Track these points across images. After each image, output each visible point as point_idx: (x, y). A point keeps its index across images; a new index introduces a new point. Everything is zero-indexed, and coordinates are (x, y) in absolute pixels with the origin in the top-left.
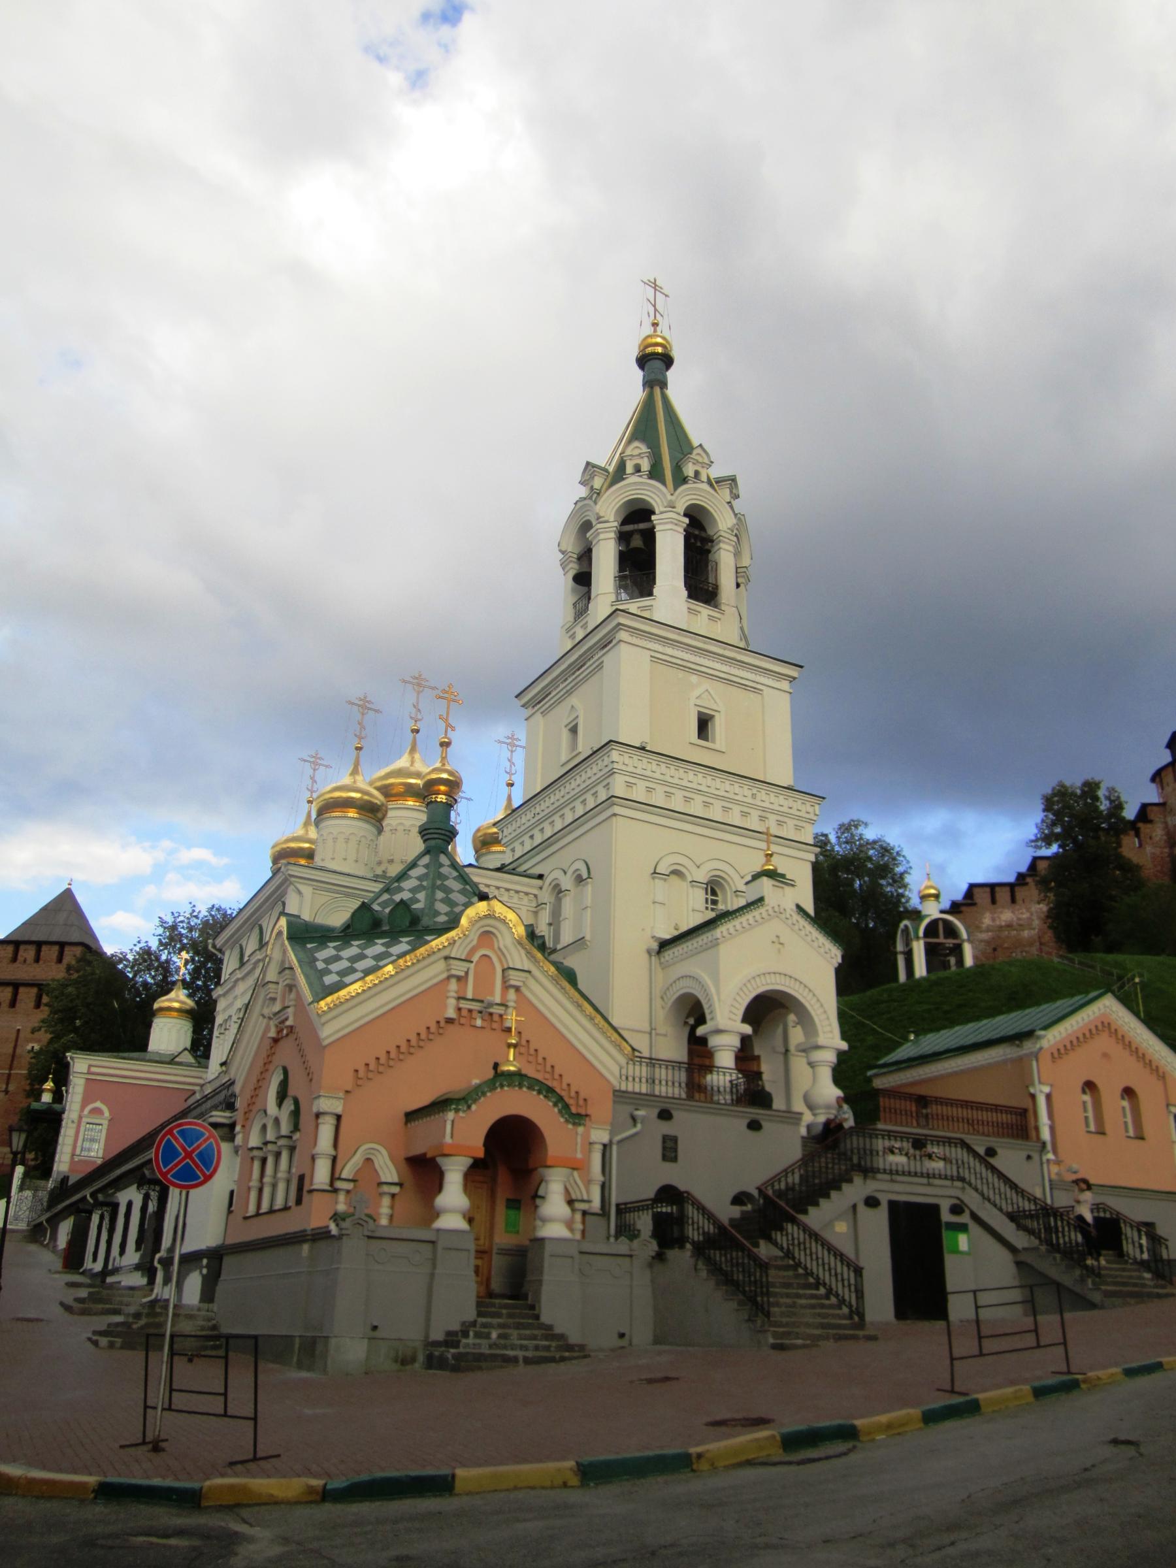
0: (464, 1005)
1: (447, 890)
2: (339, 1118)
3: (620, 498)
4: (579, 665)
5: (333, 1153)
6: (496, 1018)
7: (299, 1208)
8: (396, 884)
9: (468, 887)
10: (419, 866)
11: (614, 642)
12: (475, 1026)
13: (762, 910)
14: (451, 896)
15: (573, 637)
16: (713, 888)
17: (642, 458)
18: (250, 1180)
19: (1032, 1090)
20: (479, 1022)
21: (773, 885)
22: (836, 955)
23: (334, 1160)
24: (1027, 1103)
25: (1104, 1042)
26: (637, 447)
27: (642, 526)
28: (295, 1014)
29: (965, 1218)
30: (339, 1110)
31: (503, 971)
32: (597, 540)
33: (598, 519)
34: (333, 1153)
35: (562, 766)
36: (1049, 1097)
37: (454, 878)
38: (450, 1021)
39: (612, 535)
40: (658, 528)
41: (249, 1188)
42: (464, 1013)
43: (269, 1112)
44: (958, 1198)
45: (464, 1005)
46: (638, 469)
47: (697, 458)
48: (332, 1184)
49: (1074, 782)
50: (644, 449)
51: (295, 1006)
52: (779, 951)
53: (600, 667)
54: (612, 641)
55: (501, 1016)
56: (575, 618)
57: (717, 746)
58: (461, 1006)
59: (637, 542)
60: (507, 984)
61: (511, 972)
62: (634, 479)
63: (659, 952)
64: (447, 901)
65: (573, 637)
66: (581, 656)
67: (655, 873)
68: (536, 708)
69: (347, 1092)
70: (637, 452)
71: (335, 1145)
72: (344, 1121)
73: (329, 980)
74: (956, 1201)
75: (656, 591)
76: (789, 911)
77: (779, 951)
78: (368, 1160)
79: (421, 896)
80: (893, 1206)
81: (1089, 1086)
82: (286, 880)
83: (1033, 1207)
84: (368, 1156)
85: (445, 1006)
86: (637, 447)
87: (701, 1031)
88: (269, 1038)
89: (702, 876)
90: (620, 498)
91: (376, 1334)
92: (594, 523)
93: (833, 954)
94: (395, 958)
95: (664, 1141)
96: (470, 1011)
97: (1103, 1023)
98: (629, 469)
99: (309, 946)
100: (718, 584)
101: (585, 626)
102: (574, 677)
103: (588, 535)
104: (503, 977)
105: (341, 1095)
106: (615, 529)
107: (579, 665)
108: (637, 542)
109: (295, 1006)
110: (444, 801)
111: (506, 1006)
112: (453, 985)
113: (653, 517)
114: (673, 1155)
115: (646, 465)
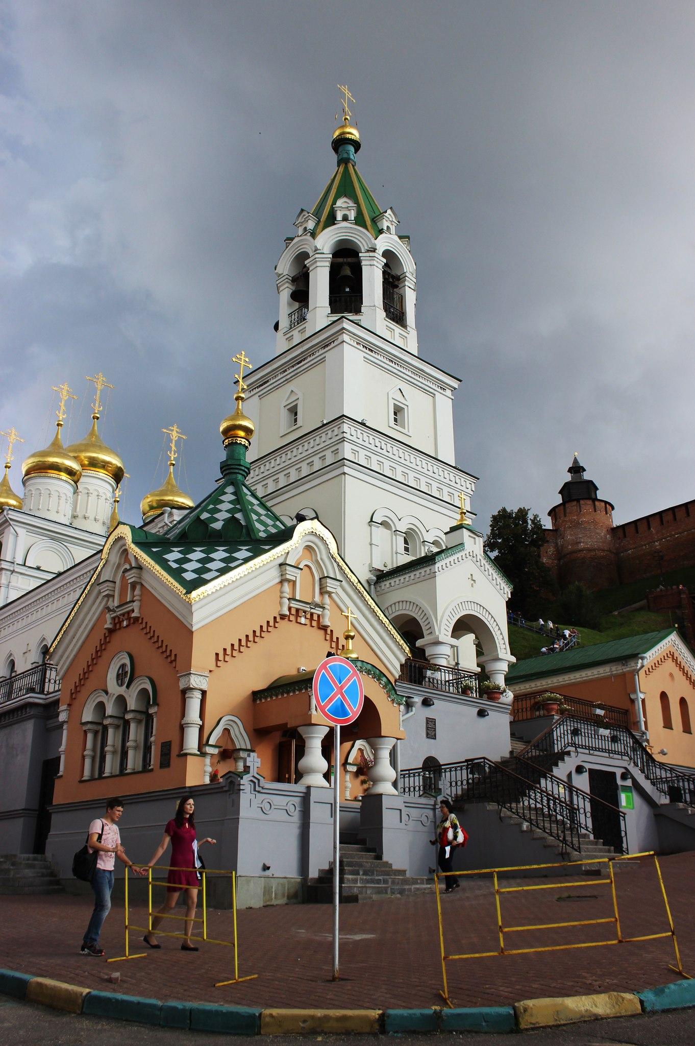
0: (294, 605)
2: (204, 693)
3: (337, 235)
4: (298, 360)
5: (201, 723)
6: (315, 617)
7: (166, 770)
9: (269, 513)
11: (336, 343)
12: (300, 623)
13: (463, 553)
14: (261, 518)
15: (290, 339)
16: (409, 537)
17: (350, 210)
18: (84, 750)
19: (633, 696)
20: (303, 620)
21: (469, 536)
22: (507, 592)
23: (201, 729)
24: (626, 705)
25: (669, 665)
26: (346, 202)
27: (350, 260)
28: (140, 607)
29: (629, 783)
30: (204, 687)
31: (320, 579)
32: (315, 266)
33: (316, 250)
34: (201, 723)
35: (281, 437)
36: (643, 701)
37: (258, 505)
38: (283, 617)
39: (328, 264)
40: (363, 263)
41: (83, 757)
42: (293, 612)
43: (110, 690)
44: (626, 768)
45: (294, 605)
46: (345, 218)
47: (389, 216)
48: (200, 749)
49: (513, 507)
50: (351, 204)
51: (140, 600)
52: (472, 586)
53: (323, 360)
54: (334, 341)
55: (319, 616)
56: (291, 325)
57: (405, 431)
58: (292, 605)
59: (347, 272)
60: (323, 591)
61: (329, 580)
62: (345, 224)
63: (376, 583)
65: (290, 339)
66: (302, 353)
67: (371, 521)
68: (252, 393)
69: (210, 671)
70: (345, 205)
71: (202, 716)
73: (189, 576)
74: (624, 770)
75: (363, 310)
76: (479, 557)
77: (472, 586)
78: (226, 731)
80: (591, 772)
81: (664, 696)
82: (6, 521)
83: (669, 775)
84: (229, 727)
86: (346, 202)
87: (419, 643)
88: (106, 629)
89: (403, 527)
90: (337, 235)
91: (268, 873)
92: (311, 254)
93: (506, 590)
94: (241, 562)
95: (427, 721)
96: (297, 610)
97: (670, 652)
98: (339, 217)
99: (154, 550)
100: (404, 311)
101: (302, 331)
102: (293, 369)
103: (306, 262)
104: (321, 584)
105: (207, 674)
106: (330, 259)
107: (298, 360)
108: (347, 272)
109: (140, 600)
110: (243, 443)
111: (324, 608)
112: (287, 588)
113: (360, 255)
114: (433, 734)
115: (352, 215)
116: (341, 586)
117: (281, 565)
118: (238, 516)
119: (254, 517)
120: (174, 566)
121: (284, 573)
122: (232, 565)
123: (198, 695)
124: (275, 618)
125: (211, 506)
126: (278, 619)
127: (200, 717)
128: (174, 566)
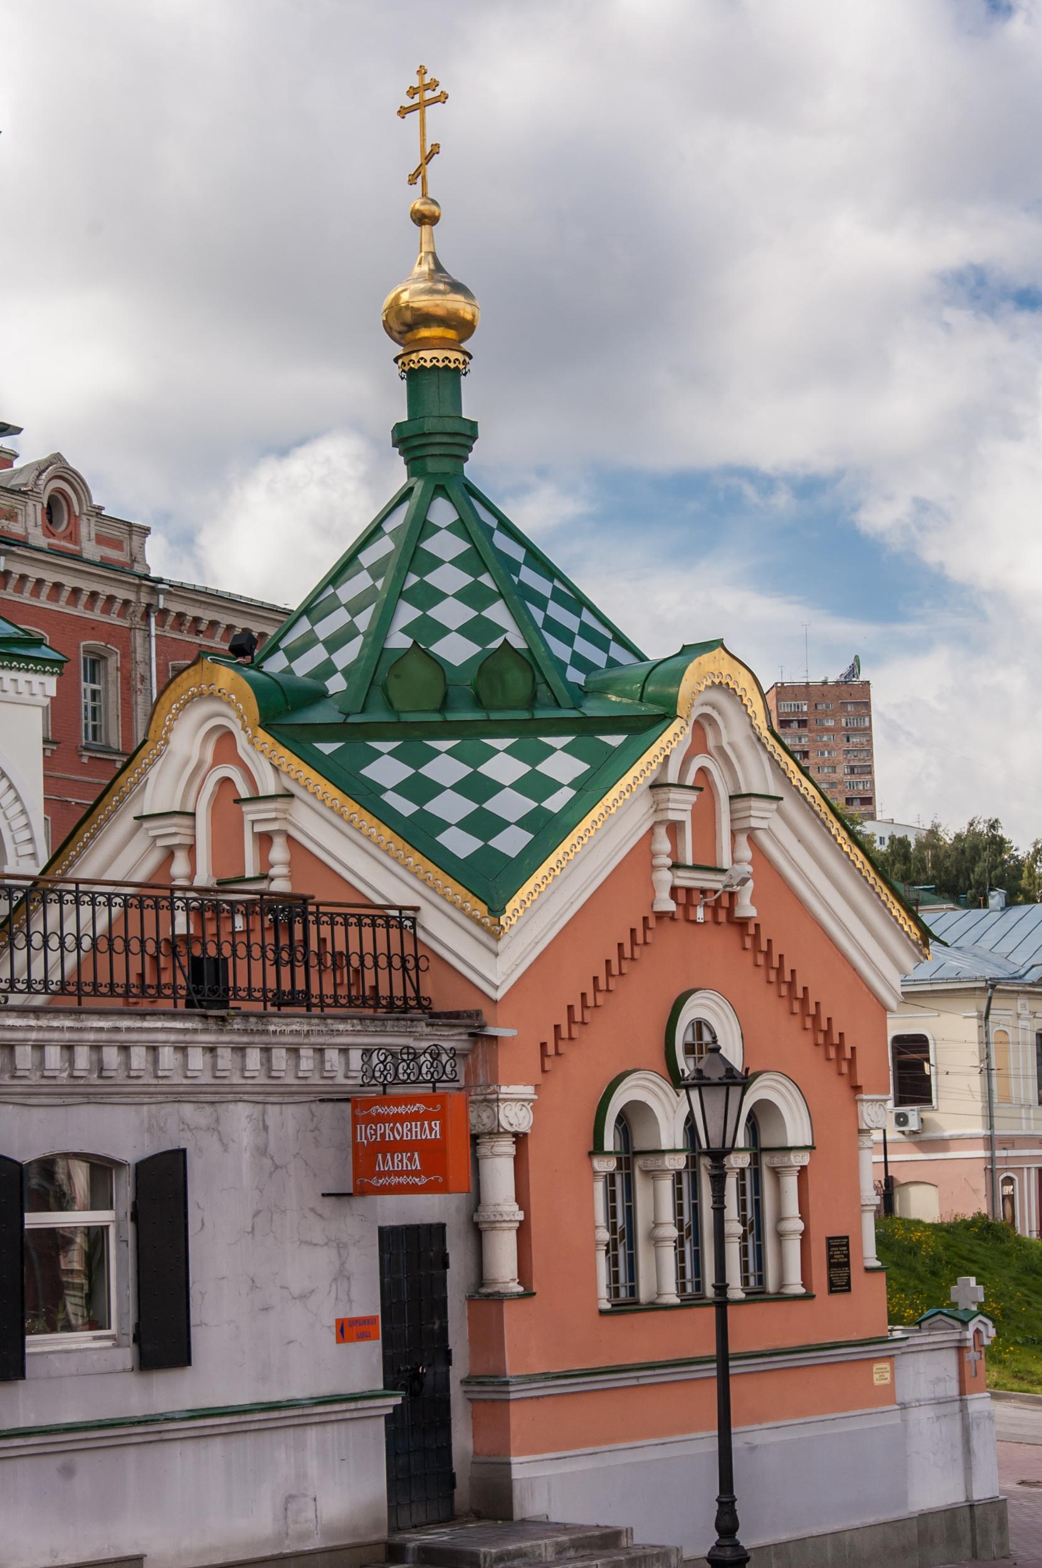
0: (685, 879)
1: (542, 603)
5: (520, 1216)
8: (413, 579)
10: (438, 529)
12: (694, 922)
20: (700, 914)
31: (731, 798)
34: (520, 1216)
38: (660, 916)
58: (679, 882)
61: (755, 803)
64: (567, 637)
72: (532, 1145)
79: (497, 613)
85: (652, 890)
96: (689, 890)
116: (779, 811)
117: (655, 786)
118: (497, 613)
119: (538, 615)
120: (406, 807)
121: (662, 806)
122: (555, 803)
123: (507, 1147)
124: (645, 919)
125: (413, 579)
126: (652, 923)
127: (518, 1199)
128: (406, 807)
